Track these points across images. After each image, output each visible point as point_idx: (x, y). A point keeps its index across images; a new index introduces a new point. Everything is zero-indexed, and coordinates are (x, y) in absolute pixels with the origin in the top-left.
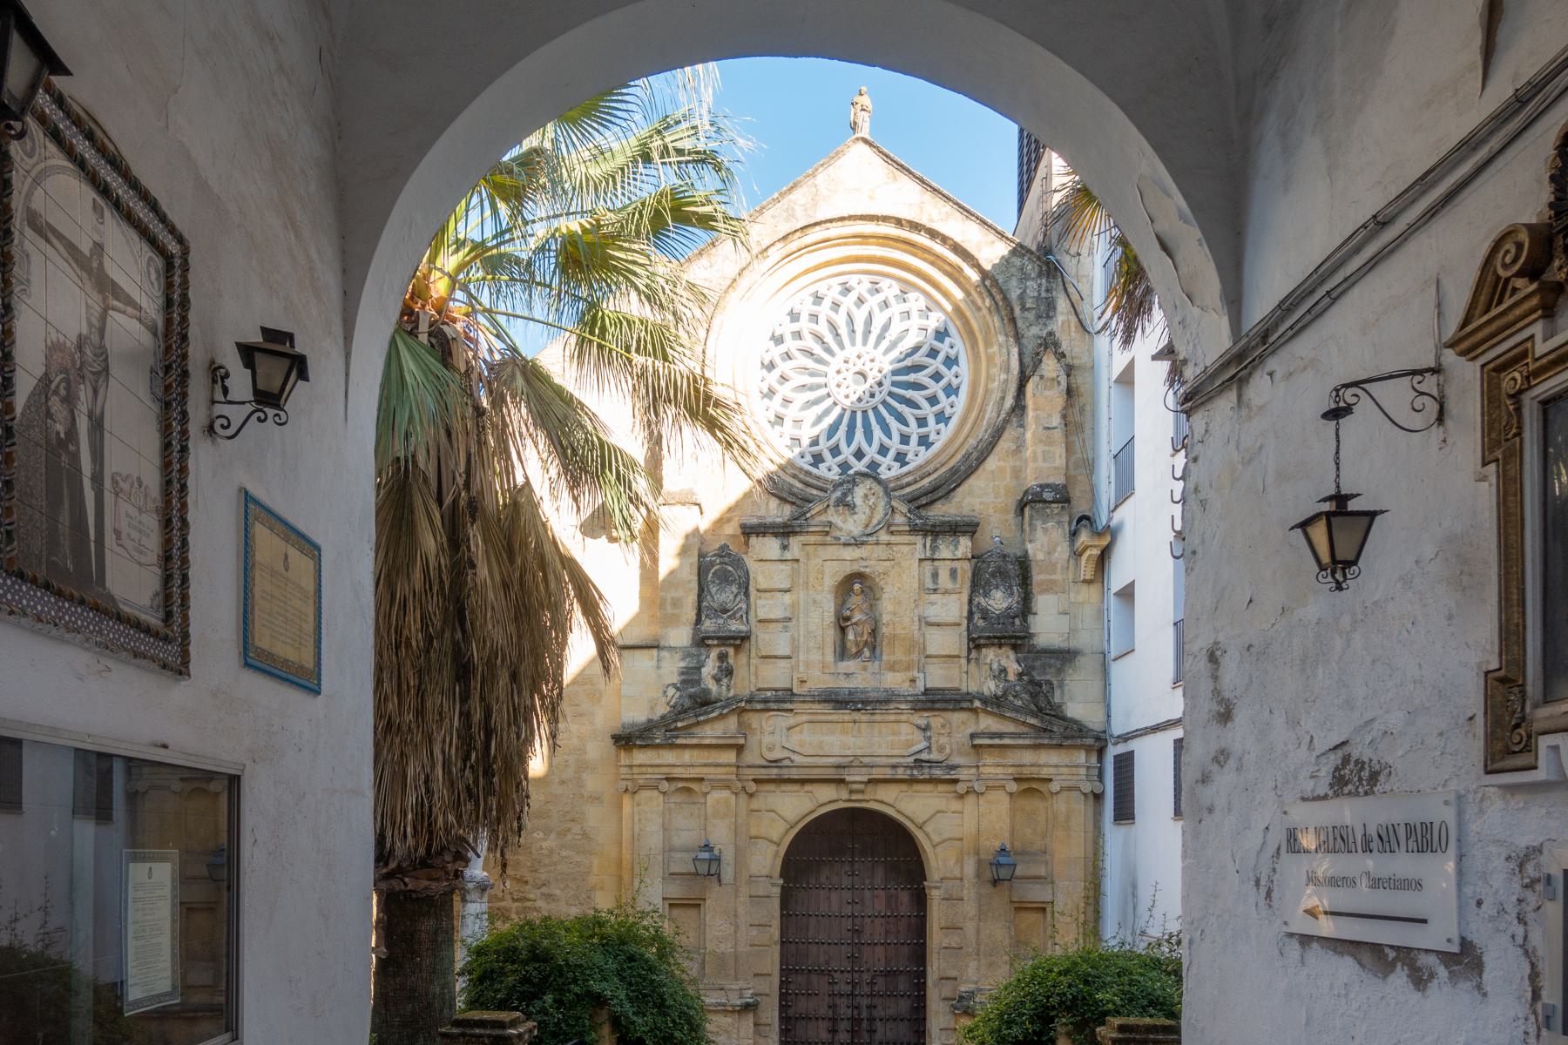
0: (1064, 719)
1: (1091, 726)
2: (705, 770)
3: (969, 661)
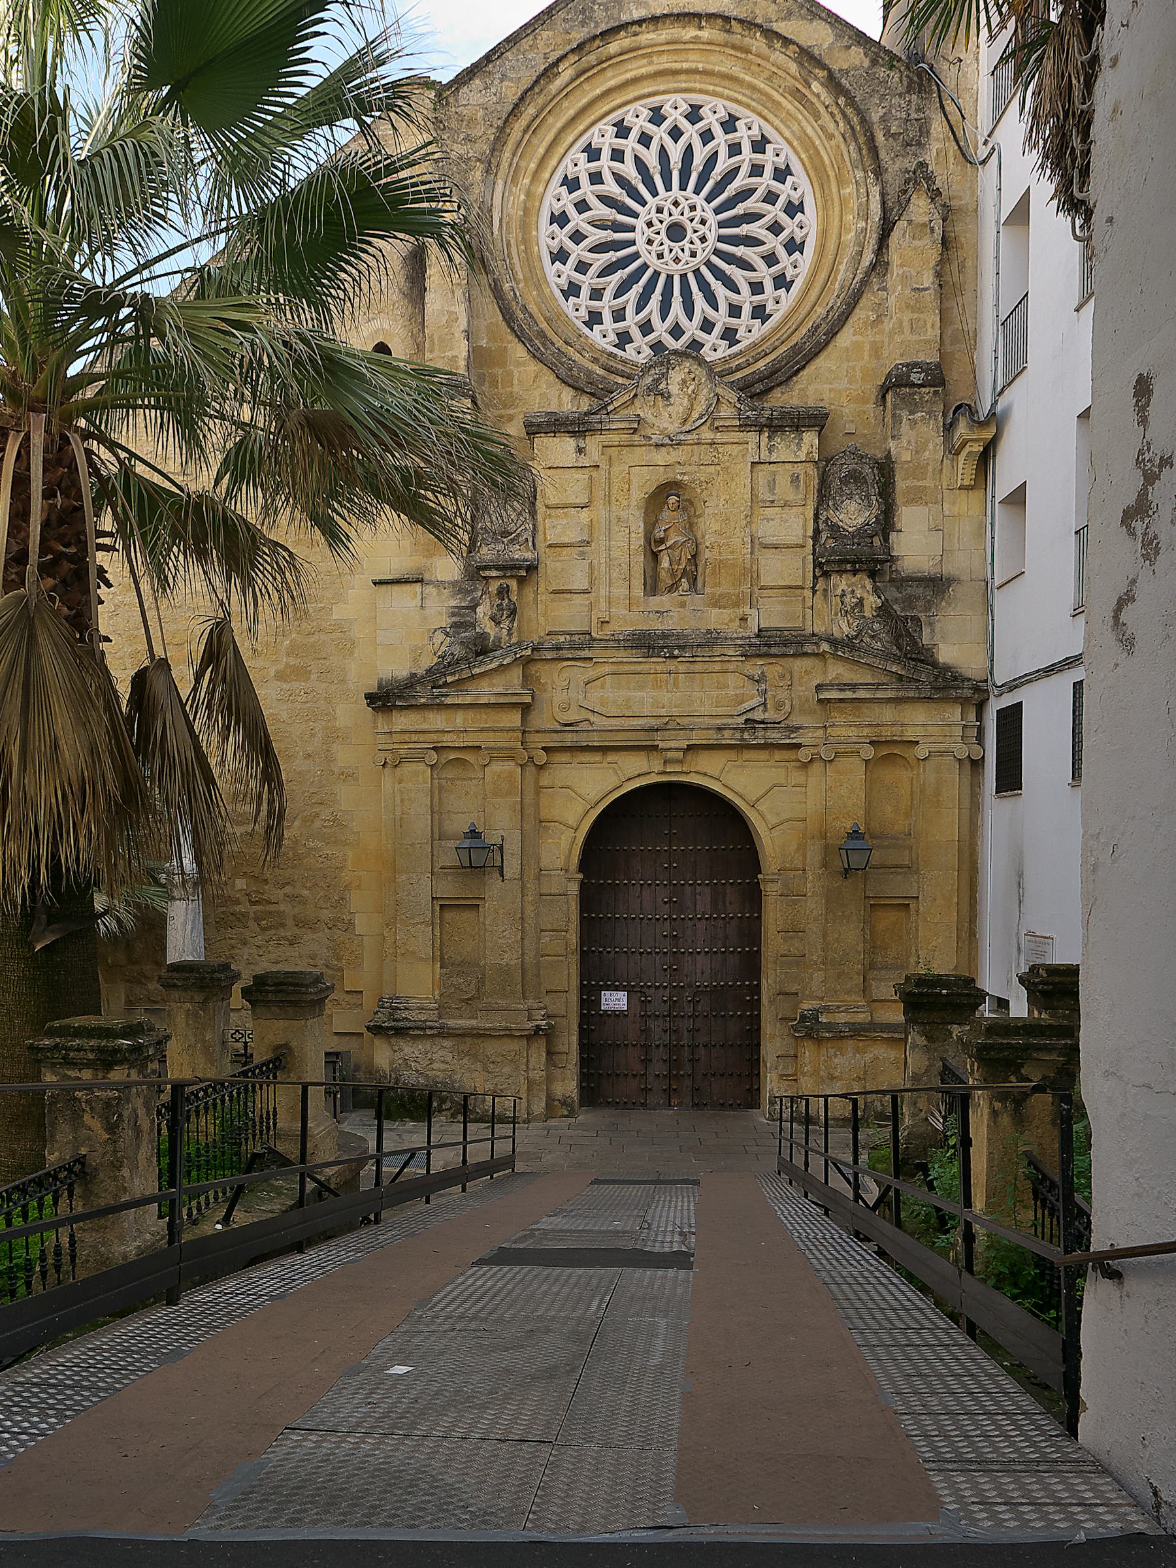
0: (934, 664)
1: (968, 673)
3: (814, 592)
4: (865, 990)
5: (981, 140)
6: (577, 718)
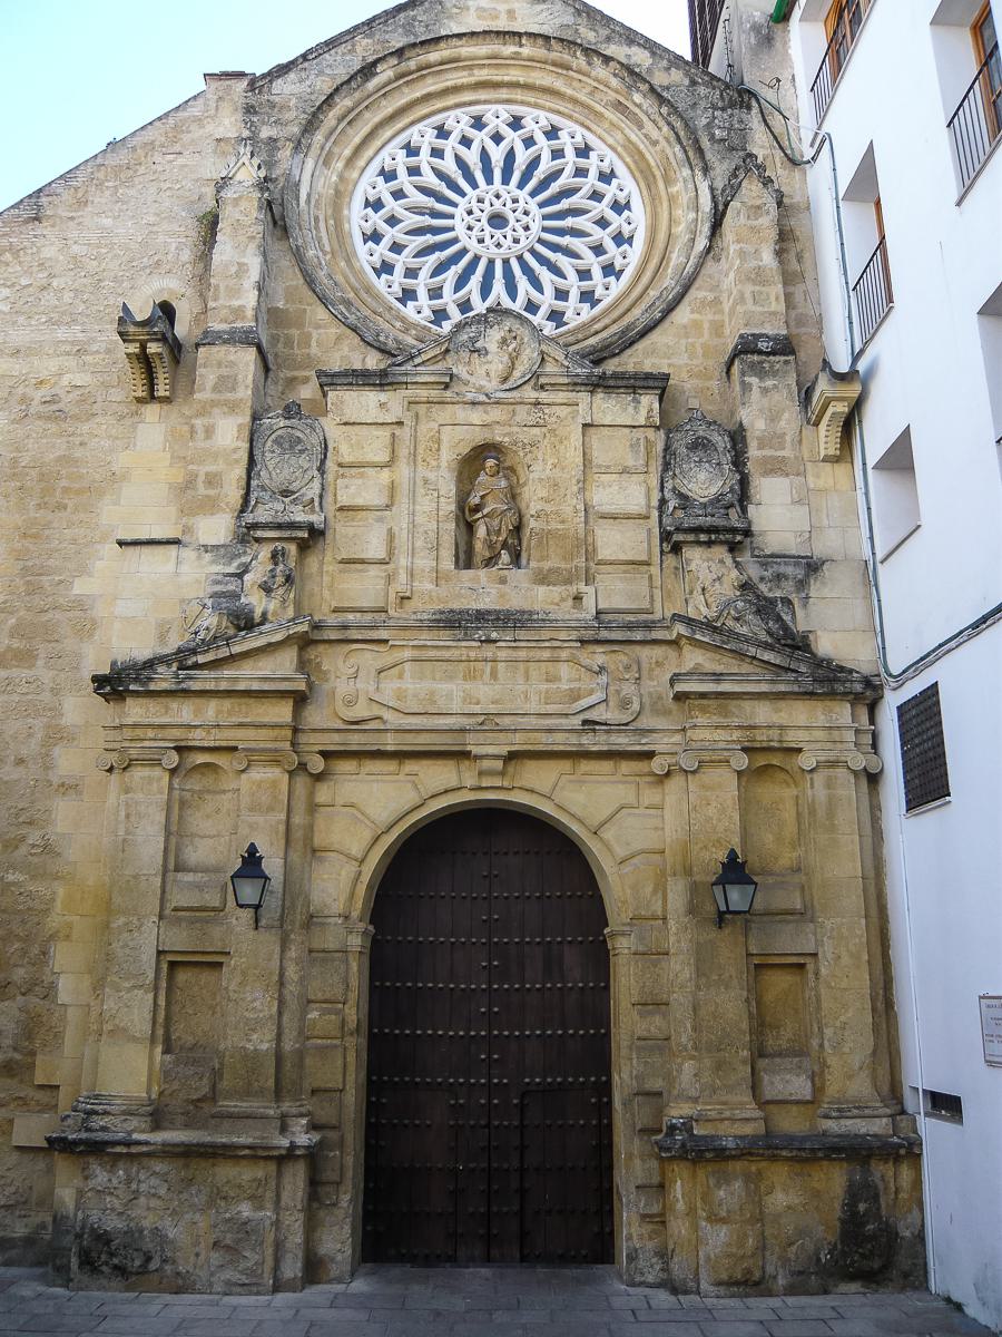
2: (241, 733)
4: (755, 1087)
5: (807, 136)
6: (365, 714)
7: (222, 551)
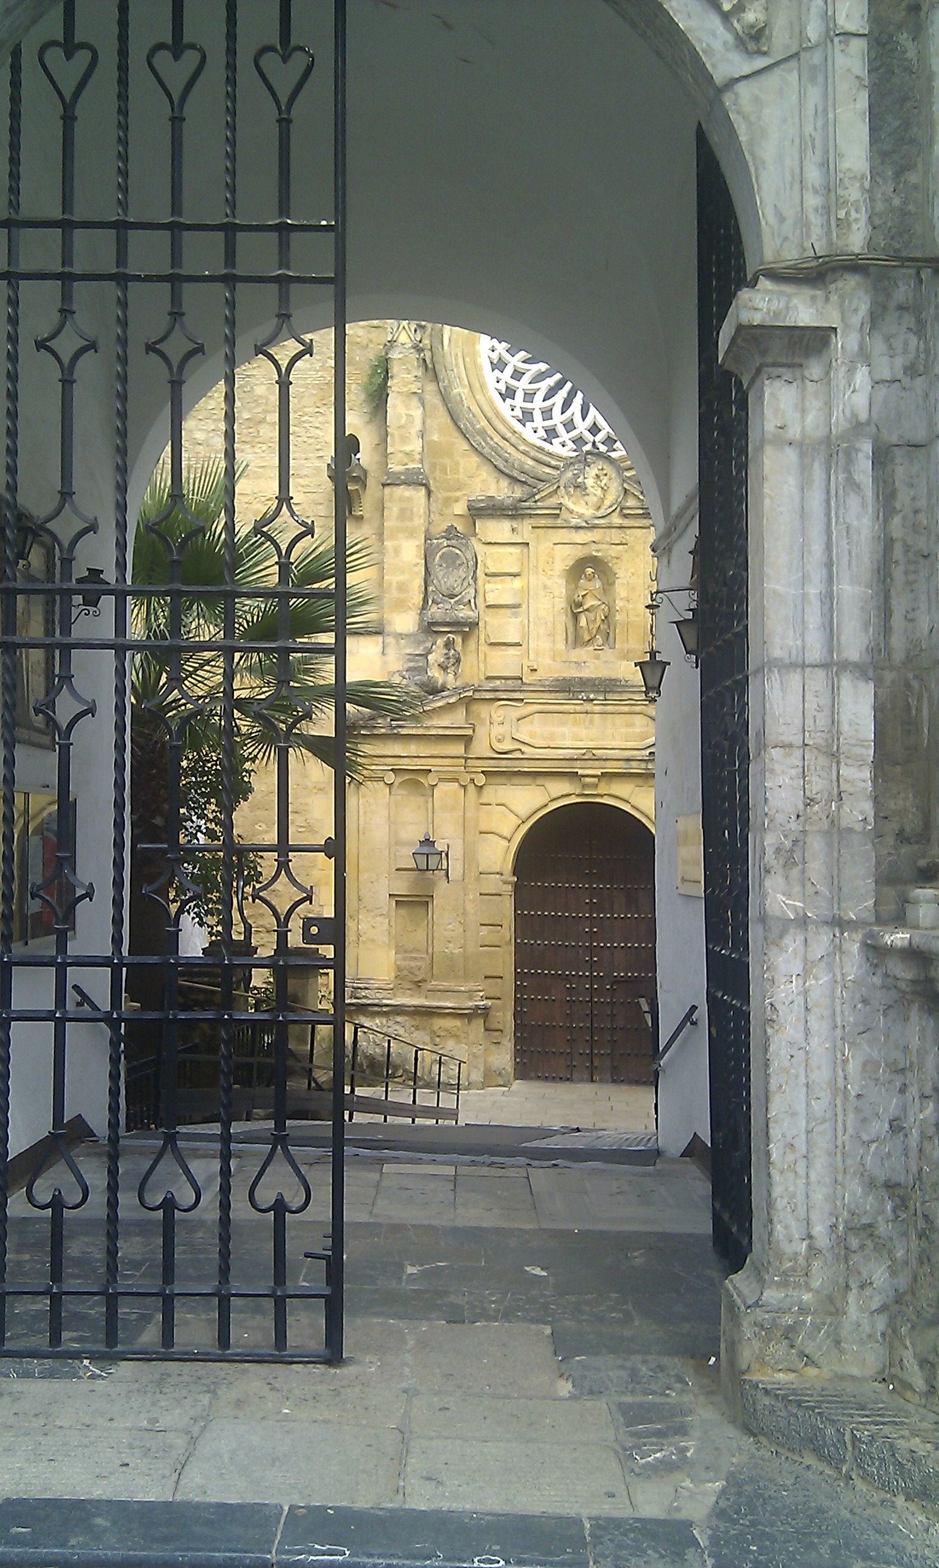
6: (511, 748)
7: (412, 639)
